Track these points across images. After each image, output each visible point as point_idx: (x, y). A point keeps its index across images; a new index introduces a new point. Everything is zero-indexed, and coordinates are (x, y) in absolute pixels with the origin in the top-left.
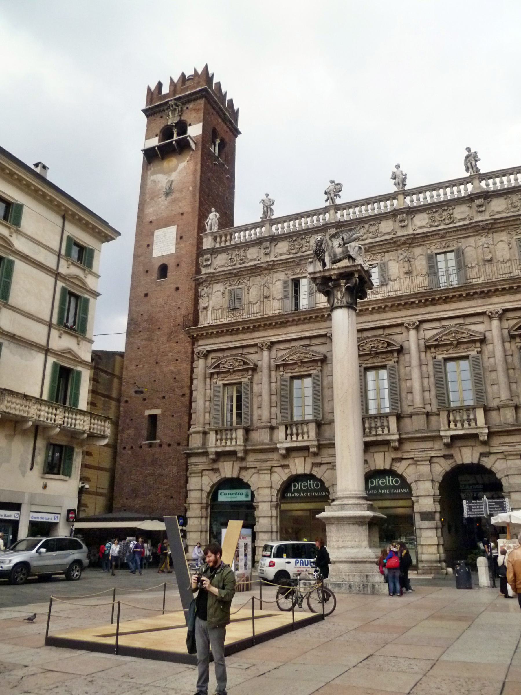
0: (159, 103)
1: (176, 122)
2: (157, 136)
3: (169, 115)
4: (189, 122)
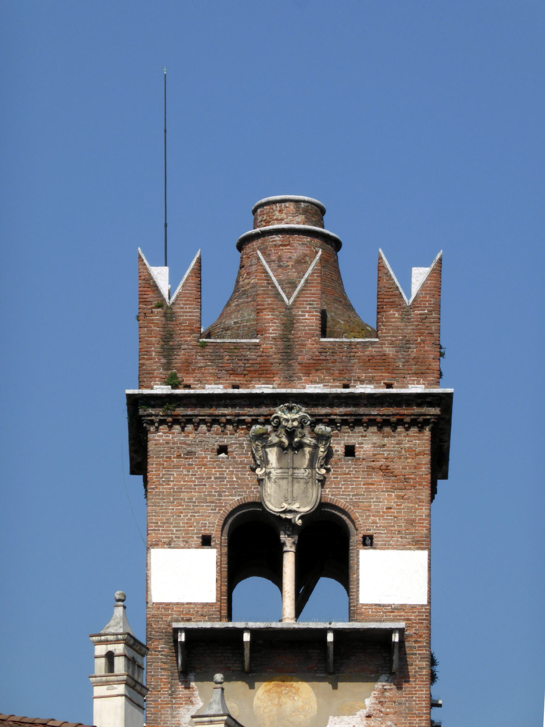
0: (217, 389)
1: (305, 509)
2: (206, 541)
3: (266, 462)
4: (362, 523)
